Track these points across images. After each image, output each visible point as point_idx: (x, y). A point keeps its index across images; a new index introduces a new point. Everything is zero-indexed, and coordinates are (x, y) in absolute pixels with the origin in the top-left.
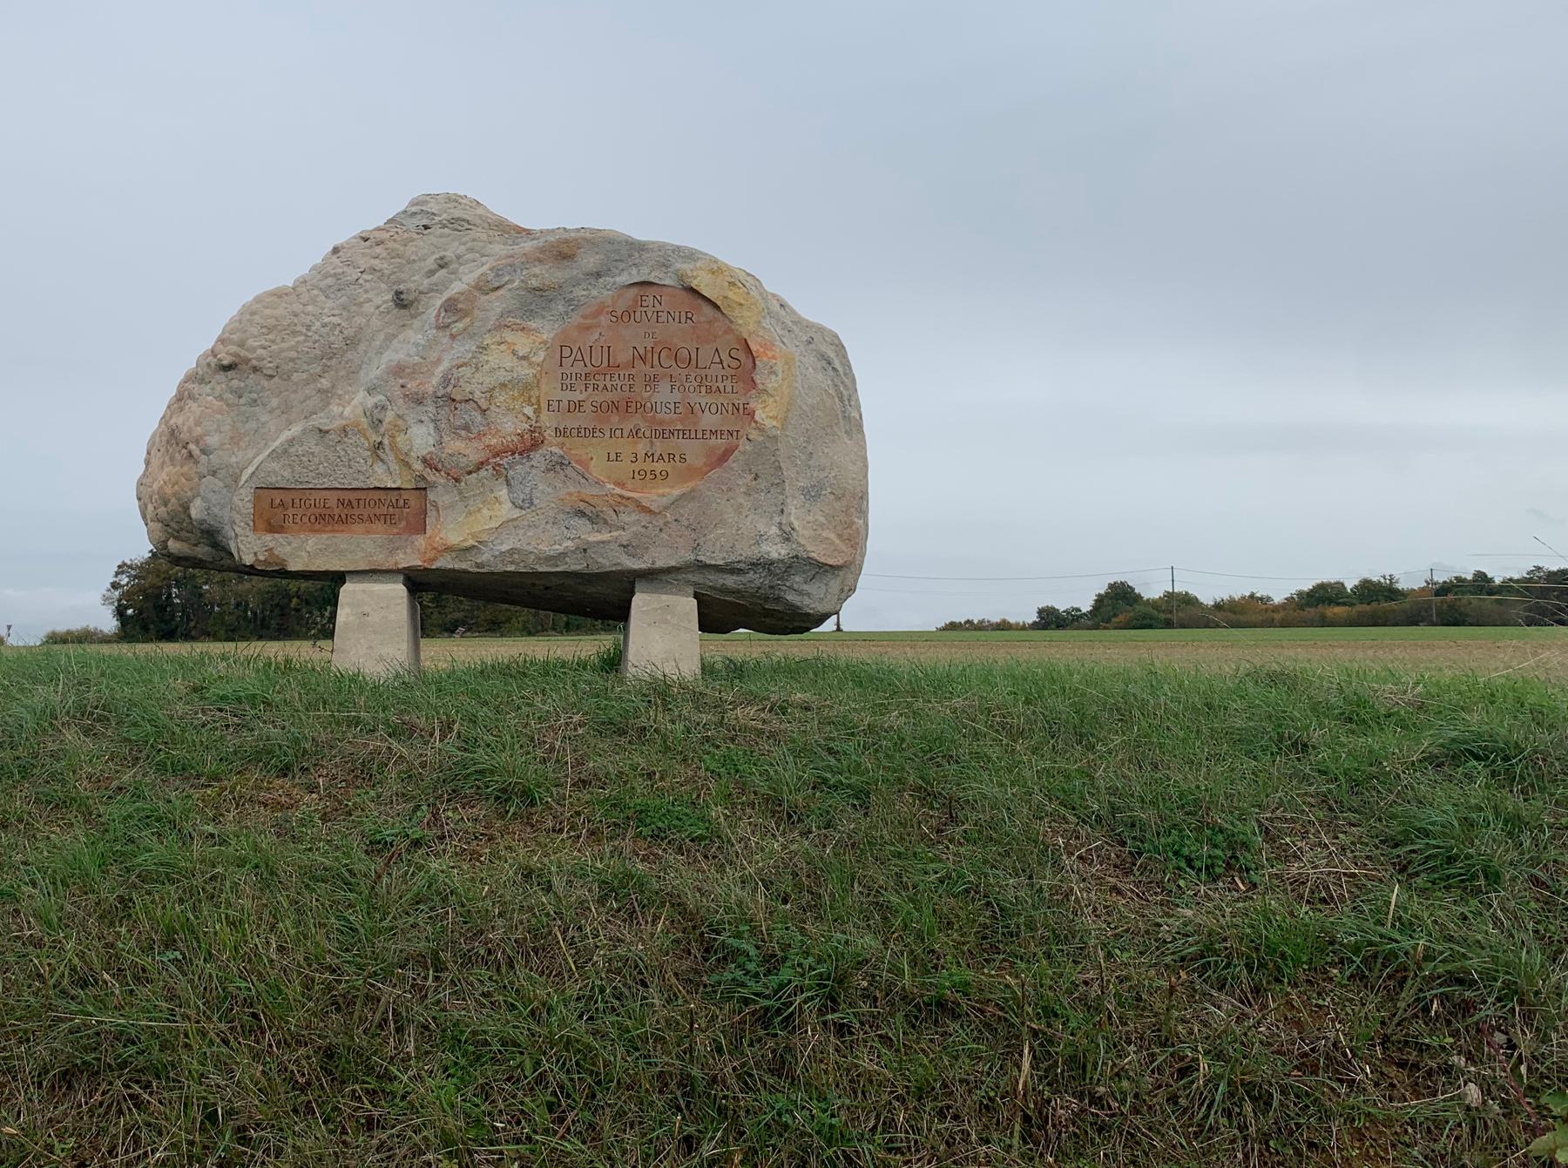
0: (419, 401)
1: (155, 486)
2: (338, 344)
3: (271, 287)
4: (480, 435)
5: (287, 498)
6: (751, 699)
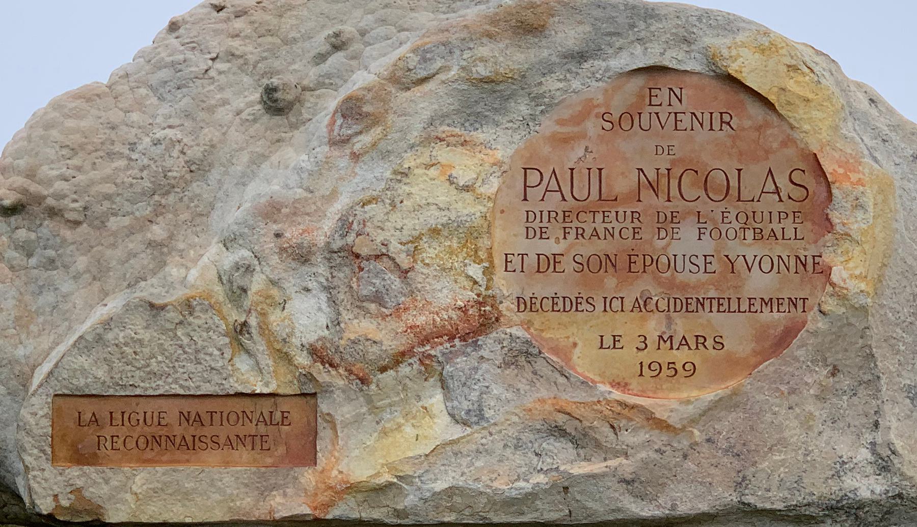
0: (302, 256)
2: (176, 166)
3: (76, 84)
4: (398, 311)
5: (103, 409)
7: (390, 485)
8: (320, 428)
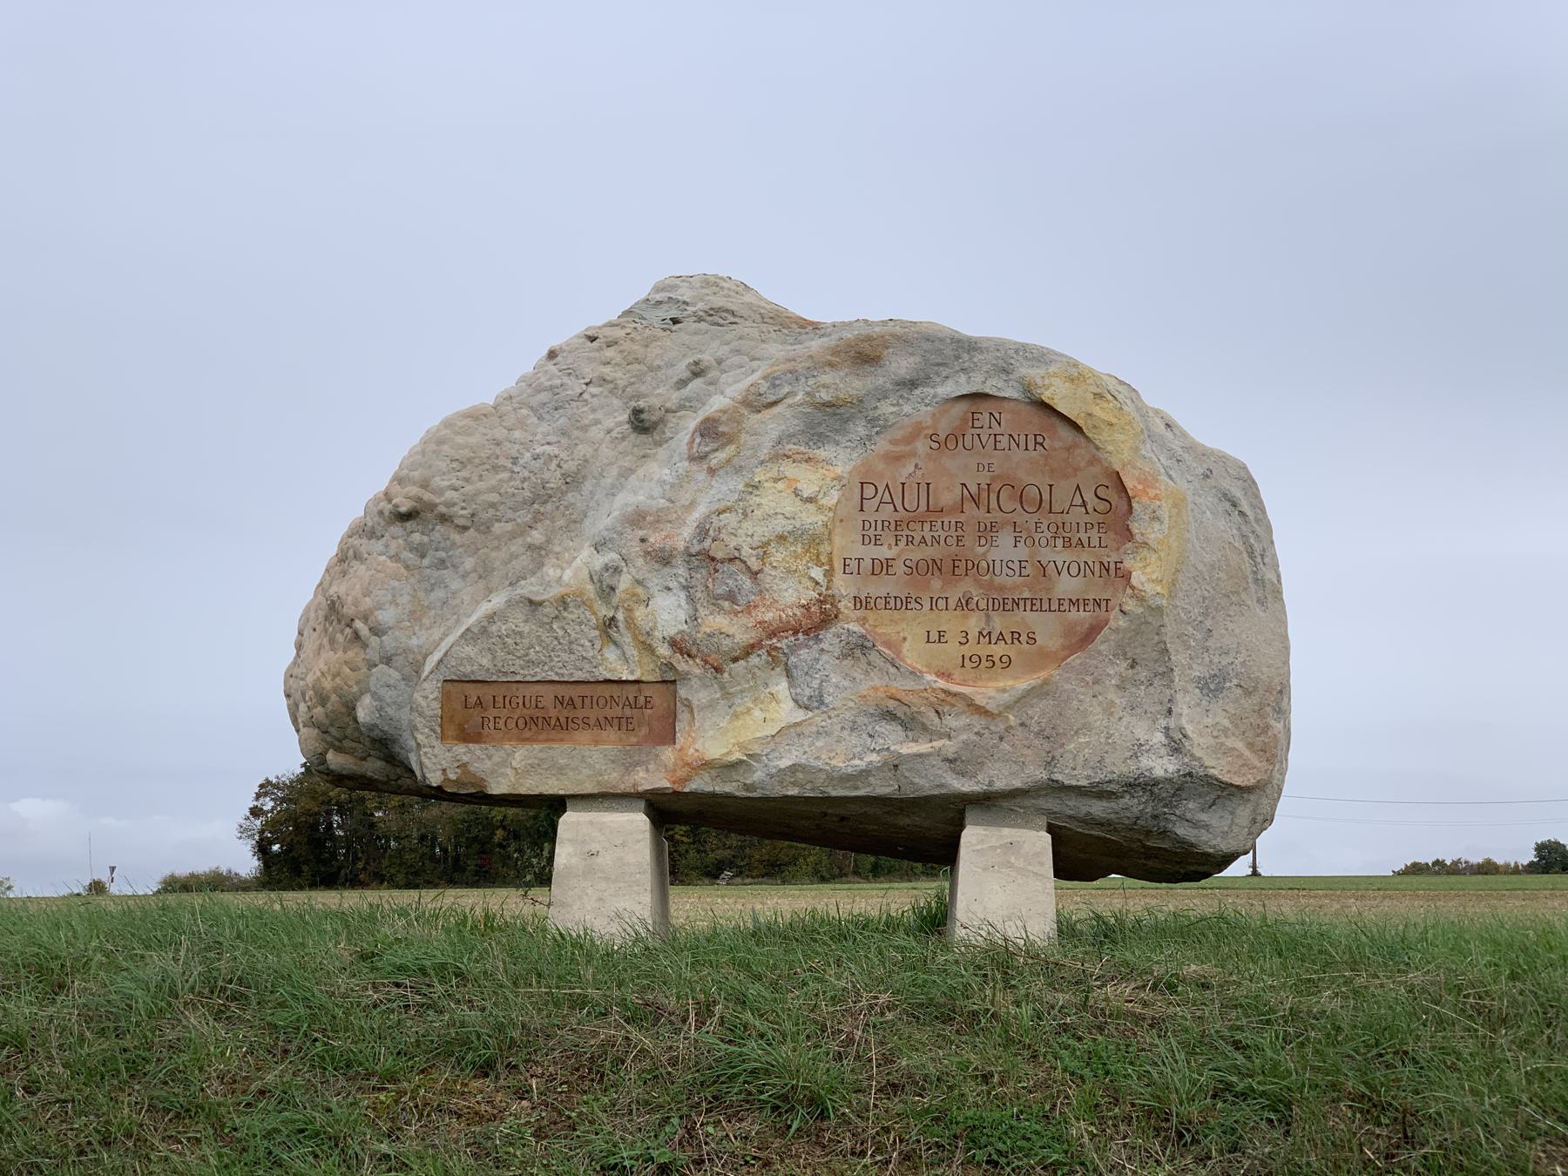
0: (663, 559)
1: (310, 679)
2: (554, 478)
3: (464, 406)
4: (749, 608)
5: (487, 693)
6: (1125, 972)
7: (741, 762)
8: (679, 712)
